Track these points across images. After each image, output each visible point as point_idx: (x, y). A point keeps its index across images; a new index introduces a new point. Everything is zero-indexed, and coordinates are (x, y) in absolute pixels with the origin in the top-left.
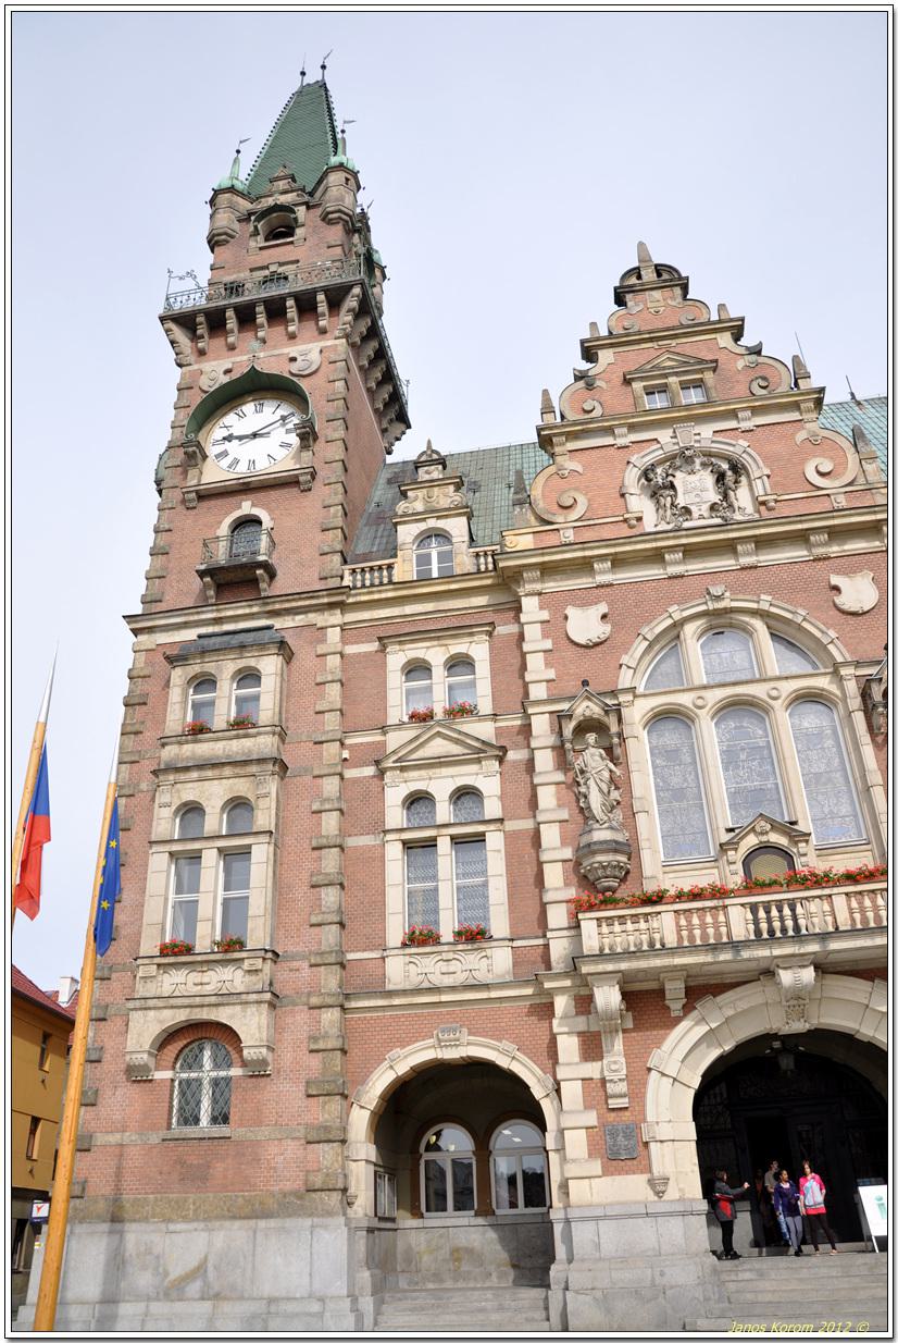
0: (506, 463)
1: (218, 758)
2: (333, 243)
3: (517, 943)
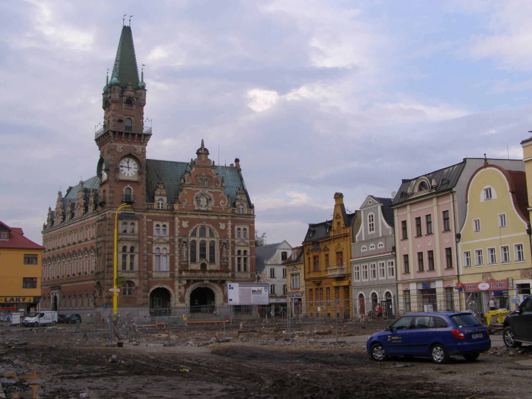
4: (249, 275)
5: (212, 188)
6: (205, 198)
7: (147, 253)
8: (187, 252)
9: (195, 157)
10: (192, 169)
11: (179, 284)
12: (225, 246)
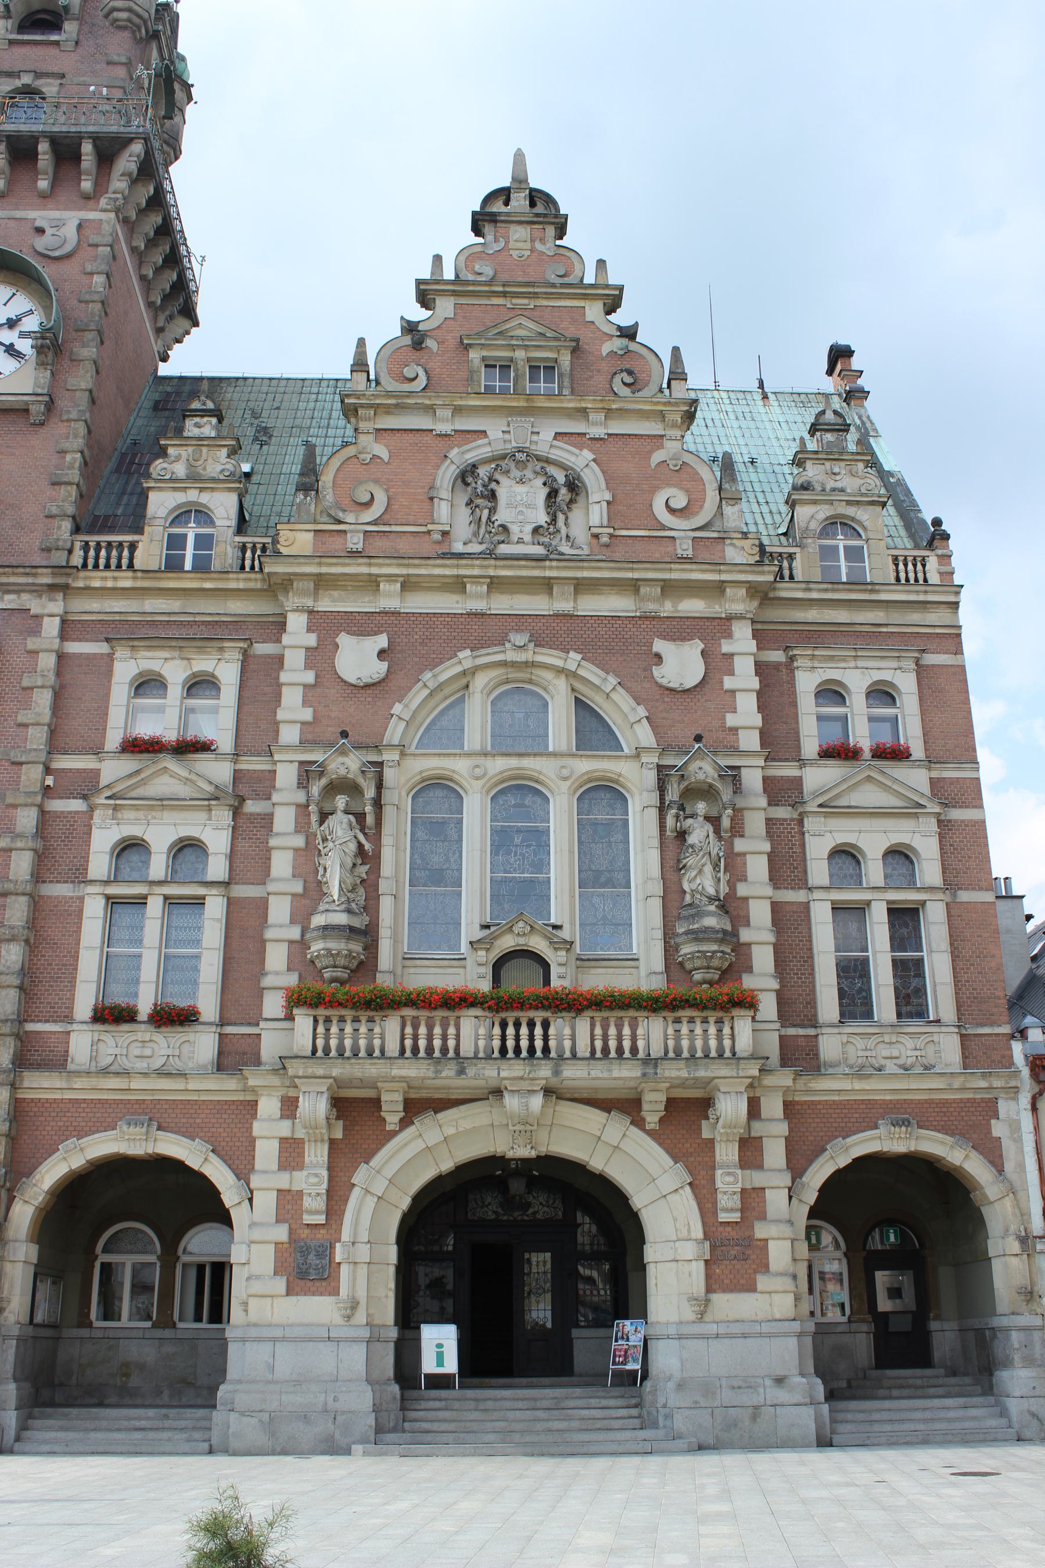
0: (312, 405)
2: (116, 58)
3: (229, 1030)
6: (539, 481)
7: (38, 877)
11: (284, 1128)
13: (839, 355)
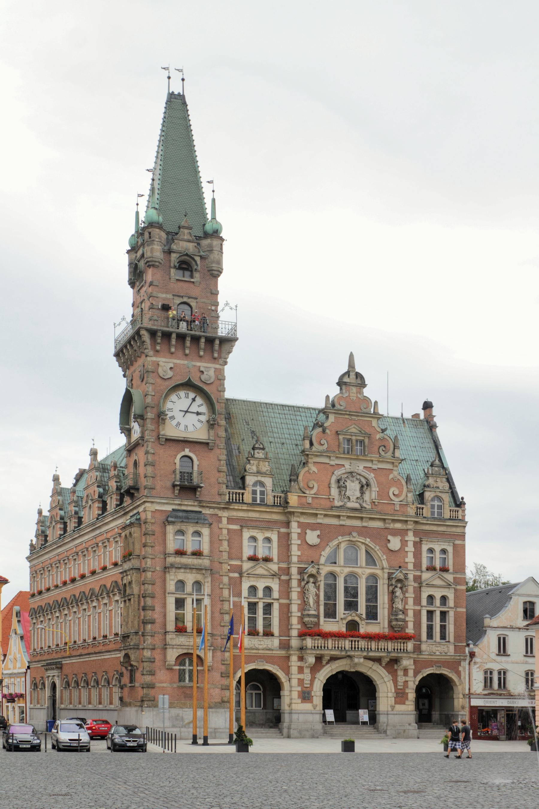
1: (189, 565)
4: (452, 648)
5: (372, 461)
6: (357, 482)
8: (318, 595)
9: (334, 391)
10: (327, 417)
11: (299, 664)
12: (399, 585)
13: (427, 406)
